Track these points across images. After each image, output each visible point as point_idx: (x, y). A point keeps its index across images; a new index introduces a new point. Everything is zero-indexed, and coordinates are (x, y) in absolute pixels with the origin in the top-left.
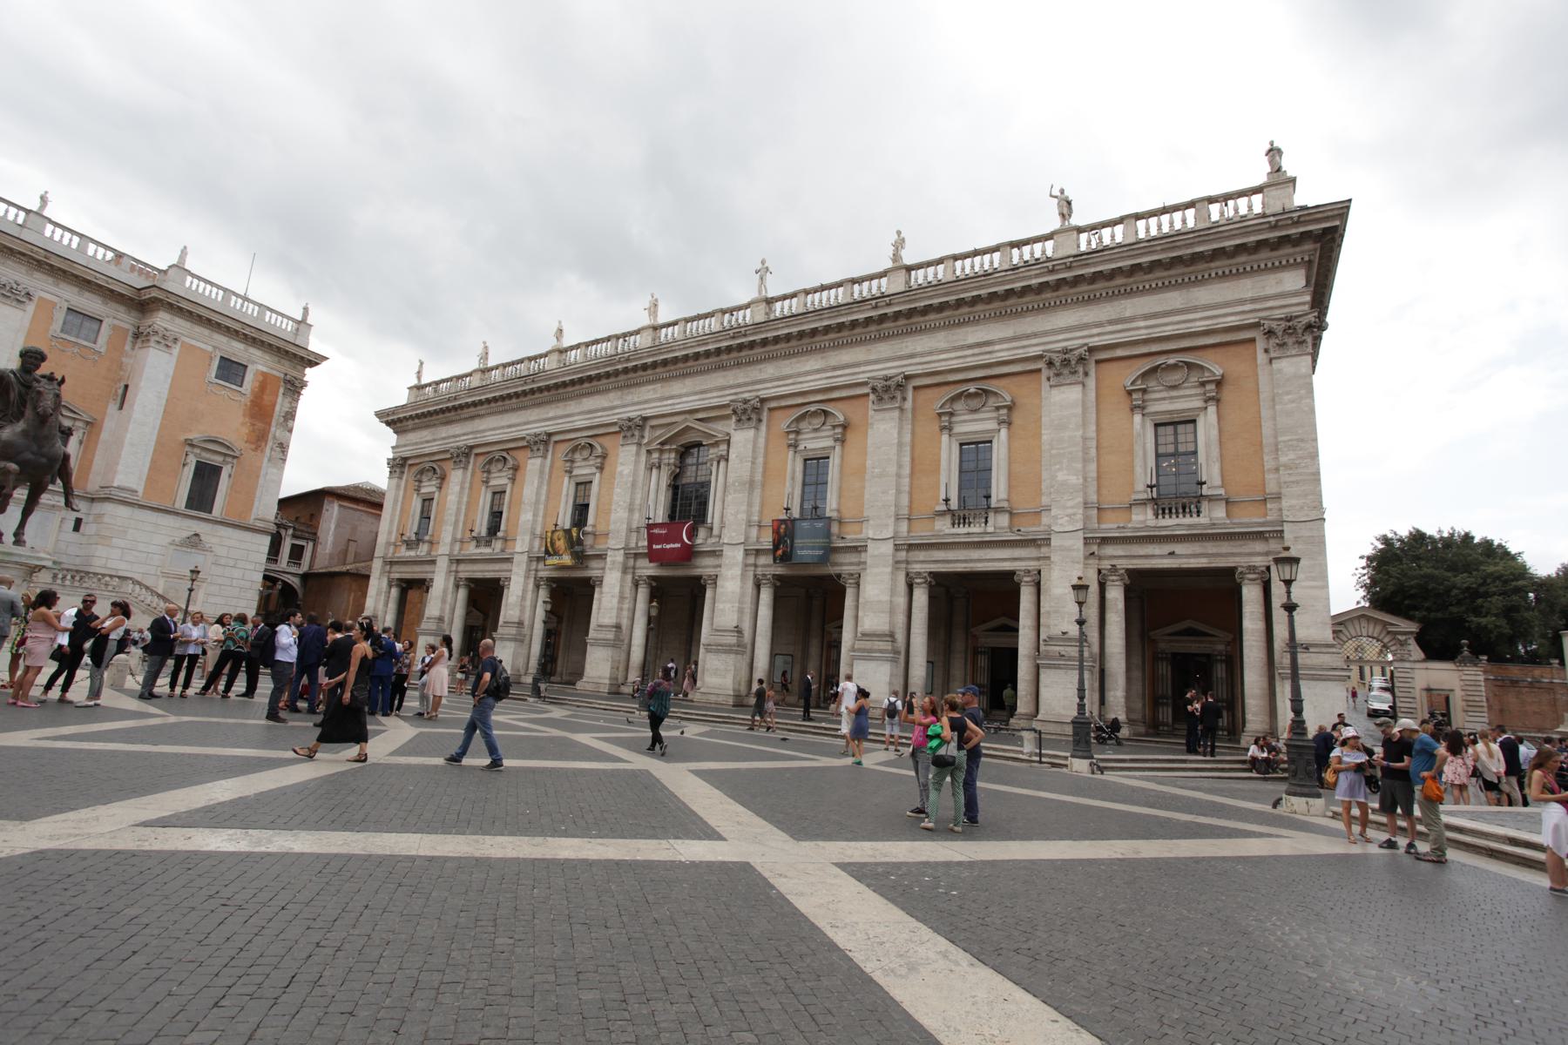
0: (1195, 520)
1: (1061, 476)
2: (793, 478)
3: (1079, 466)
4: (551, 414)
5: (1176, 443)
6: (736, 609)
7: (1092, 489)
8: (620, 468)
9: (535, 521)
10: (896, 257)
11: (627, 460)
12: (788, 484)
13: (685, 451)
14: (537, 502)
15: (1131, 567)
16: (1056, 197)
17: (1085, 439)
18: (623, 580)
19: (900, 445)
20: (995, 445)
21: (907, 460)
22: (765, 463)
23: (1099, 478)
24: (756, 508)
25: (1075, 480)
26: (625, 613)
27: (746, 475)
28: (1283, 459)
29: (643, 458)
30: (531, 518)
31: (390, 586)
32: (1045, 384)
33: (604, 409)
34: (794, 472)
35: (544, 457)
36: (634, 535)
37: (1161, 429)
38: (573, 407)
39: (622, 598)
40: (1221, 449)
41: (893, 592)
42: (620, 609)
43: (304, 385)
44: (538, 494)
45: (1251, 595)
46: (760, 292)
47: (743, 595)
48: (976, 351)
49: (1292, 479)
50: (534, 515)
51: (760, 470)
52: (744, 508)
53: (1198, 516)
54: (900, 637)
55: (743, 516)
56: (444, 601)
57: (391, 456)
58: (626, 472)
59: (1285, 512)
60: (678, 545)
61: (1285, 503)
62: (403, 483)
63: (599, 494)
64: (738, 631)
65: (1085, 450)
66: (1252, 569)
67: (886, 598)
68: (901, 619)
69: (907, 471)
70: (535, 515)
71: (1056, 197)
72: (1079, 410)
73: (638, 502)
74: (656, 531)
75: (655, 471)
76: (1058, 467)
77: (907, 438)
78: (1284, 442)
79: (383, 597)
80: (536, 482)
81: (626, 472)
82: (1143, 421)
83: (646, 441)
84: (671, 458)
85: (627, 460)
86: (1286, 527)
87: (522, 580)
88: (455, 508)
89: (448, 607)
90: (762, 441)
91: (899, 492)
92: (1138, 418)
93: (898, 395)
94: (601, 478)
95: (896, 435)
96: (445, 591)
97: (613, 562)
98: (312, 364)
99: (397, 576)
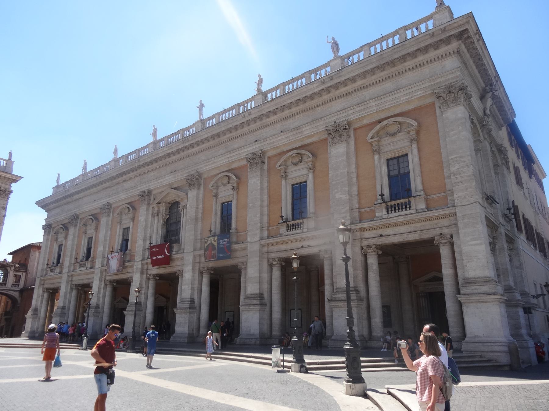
0: (408, 212)
1: (338, 196)
2: (216, 214)
3: (347, 189)
5: (399, 168)
6: (190, 288)
10: (259, 90)
12: (213, 217)
14: (105, 240)
15: (378, 243)
16: (330, 42)
18: (141, 278)
19: (262, 189)
20: (308, 183)
21: (266, 197)
23: (359, 195)
25: (345, 197)
28: (453, 169)
29: (151, 212)
30: (102, 249)
31: (44, 292)
34: (216, 210)
35: (109, 216)
37: (391, 162)
40: (421, 168)
41: (261, 271)
43: (11, 192)
45: (445, 252)
46: (200, 117)
48: (294, 132)
49: (458, 180)
50: (104, 247)
51: (201, 211)
52: (193, 233)
53: (410, 209)
55: (192, 237)
57: (44, 224)
58: (142, 220)
59: (456, 201)
60: (163, 256)
62: (50, 237)
67: (257, 275)
68: (266, 286)
69: (266, 203)
71: (330, 42)
72: (345, 158)
74: (154, 250)
75: (156, 217)
76: (336, 191)
77: (266, 185)
78: (452, 159)
79: (40, 299)
80: (104, 230)
82: (380, 159)
84: (163, 208)
85: (143, 214)
86: (458, 210)
87: (98, 283)
88: (70, 247)
89: (67, 300)
90: (201, 196)
91: (262, 215)
92: (376, 157)
95: (259, 182)
96: (66, 292)
97: (137, 268)
98: (15, 181)
99: (46, 286)
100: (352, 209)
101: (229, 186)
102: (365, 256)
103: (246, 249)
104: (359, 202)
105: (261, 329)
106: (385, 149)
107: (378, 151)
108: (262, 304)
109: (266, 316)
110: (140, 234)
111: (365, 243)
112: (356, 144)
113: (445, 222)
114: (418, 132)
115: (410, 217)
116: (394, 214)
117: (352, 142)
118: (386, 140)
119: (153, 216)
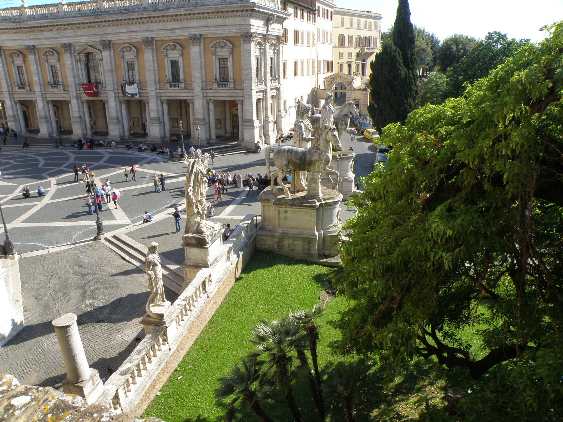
1: (196, 74)
4: (32, 37)
7: (204, 77)
8: (66, 62)
9: (39, 80)
11: (67, 59)
13: (88, 55)
17: (201, 63)
18: (78, 102)
19: (153, 60)
21: (156, 65)
22: (115, 63)
24: (115, 78)
25: (199, 75)
26: (82, 113)
27: (110, 68)
28: (245, 73)
29: (74, 58)
32: (191, 44)
33: (53, 38)
36: (77, 86)
38: (40, 35)
39: (79, 108)
41: (157, 106)
42: (79, 111)
44: (37, 69)
47: (116, 106)
52: (111, 79)
54: (161, 118)
55: (111, 82)
56: (13, 109)
58: (69, 64)
61: (245, 85)
63: (61, 70)
64: (118, 118)
65: (201, 66)
66: (240, 101)
67: (155, 108)
68: (160, 113)
69: (156, 69)
70: (39, 78)
72: (199, 54)
73: (76, 74)
77: (155, 58)
81: (69, 64)
83: (73, 52)
84: (83, 57)
85: (67, 59)
90: (112, 55)
91: (155, 75)
93: (151, 44)
94: (60, 64)
95: (151, 56)
100: (202, 81)
101: (131, 53)
102: (208, 104)
103: (148, 93)
104: (206, 78)
105: (160, 134)
106: (218, 54)
107: (215, 54)
108: (160, 123)
109: (162, 127)
110: (69, 73)
111: (208, 98)
112: (204, 46)
113: (241, 95)
114: (233, 49)
115: (227, 91)
116: (221, 88)
117: (202, 45)
118: (219, 49)
119: (77, 61)
